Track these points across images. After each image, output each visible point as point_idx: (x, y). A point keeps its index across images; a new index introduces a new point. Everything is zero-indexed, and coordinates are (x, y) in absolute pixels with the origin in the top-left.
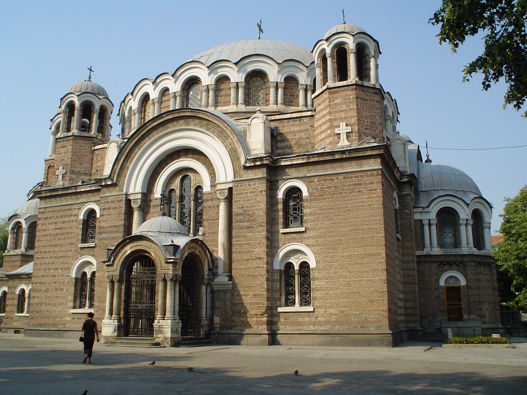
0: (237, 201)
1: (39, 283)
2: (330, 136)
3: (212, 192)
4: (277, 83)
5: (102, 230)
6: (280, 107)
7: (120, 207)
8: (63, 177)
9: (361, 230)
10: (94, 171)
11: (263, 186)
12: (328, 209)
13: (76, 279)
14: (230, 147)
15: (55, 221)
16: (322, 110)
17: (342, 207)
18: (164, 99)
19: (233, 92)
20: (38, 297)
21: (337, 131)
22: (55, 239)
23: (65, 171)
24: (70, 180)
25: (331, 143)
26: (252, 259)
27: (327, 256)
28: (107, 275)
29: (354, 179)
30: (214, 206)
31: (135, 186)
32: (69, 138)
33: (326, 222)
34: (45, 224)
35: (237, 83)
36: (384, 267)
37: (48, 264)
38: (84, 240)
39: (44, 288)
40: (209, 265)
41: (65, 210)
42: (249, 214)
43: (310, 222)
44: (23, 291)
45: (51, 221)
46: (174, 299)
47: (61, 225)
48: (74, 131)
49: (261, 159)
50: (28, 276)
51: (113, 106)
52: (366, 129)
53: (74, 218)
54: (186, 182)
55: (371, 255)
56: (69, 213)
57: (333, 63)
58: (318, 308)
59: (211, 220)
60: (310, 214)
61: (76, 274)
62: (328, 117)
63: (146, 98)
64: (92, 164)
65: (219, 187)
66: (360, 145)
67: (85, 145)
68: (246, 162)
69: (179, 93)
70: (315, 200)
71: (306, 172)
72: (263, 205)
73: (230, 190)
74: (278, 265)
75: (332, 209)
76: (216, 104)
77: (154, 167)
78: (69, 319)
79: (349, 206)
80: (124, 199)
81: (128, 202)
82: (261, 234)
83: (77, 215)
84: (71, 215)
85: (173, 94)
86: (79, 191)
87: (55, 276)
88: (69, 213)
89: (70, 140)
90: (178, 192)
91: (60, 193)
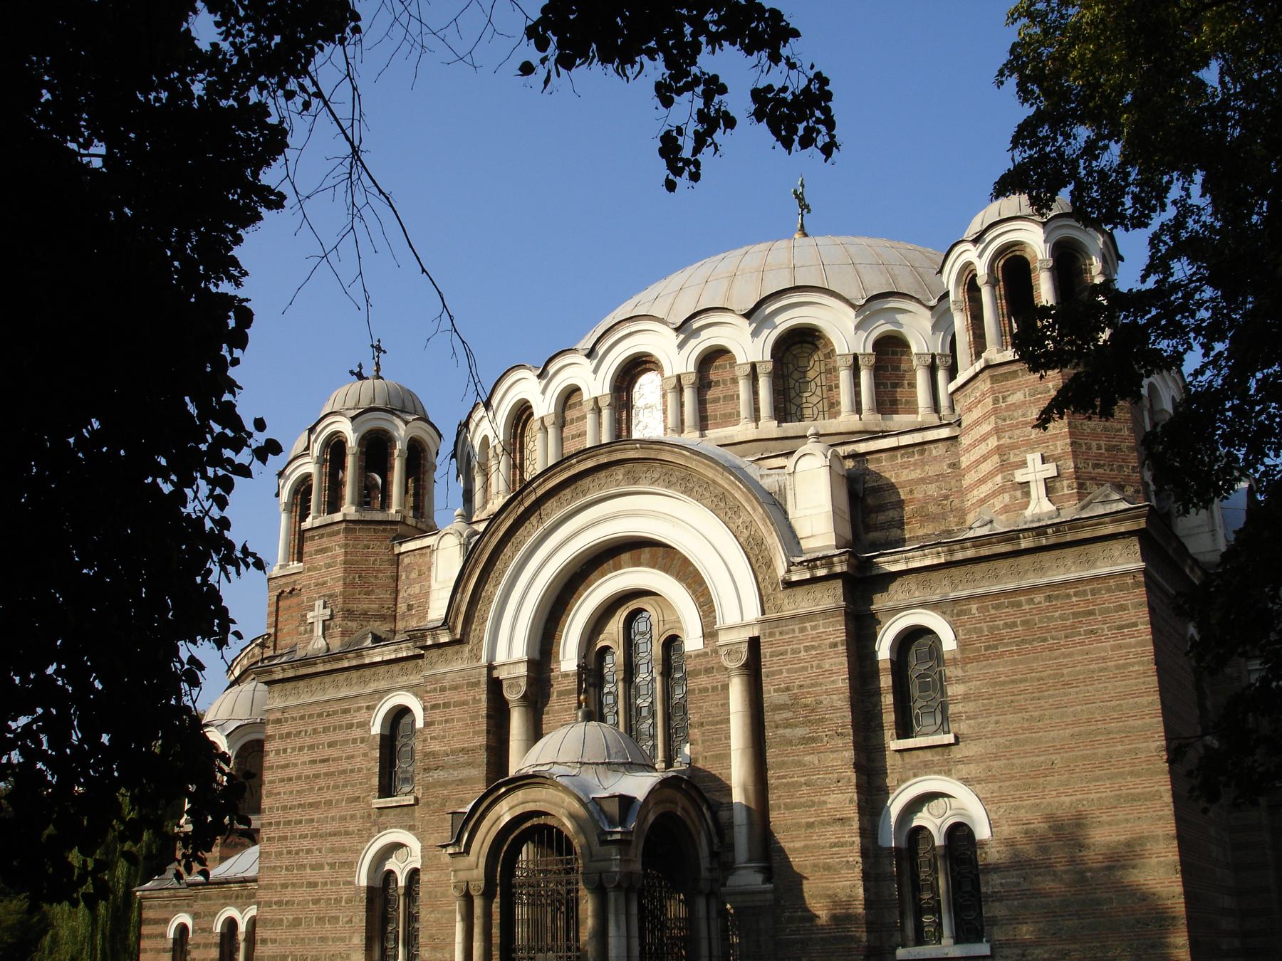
0: (773, 673)
1: (276, 903)
2: (1002, 490)
3: (708, 650)
4: (856, 357)
5: (432, 762)
6: (870, 418)
7: (475, 701)
8: (325, 628)
9: (1101, 734)
10: (402, 607)
11: (837, 631)
12: (1013, 681)
13: (370, 889)
14: (746, 533)
15: (309, 741)
16: (977, 423)
17: (1049, 676)
18: (569, 415)
19: (743, 389)
21: (1020, 476)
22: (312, 789)
23: (328, 611)
24: (343, 634)
25: (1006, 509)
26: (823, 823)
27: (1017, 808)
28: (453, 879)
29: (1074, 599)
30: (714, 689)
31: (511, 646)
32: (335, 528)
33: (1009, 717)
34: (285, 751)
35: (754, 366)
36: (1171, 829)
37: (297, 853)
38: (386, 789)
39: (288, 916)
40: (710, 843)
41: (335, 713)
42: (806, 706)
43: (968, 718)
44: (231, 924)
45: (298, 742)
46: (629, 937)
47: (326, 753)
48: (349, 509)
49: (827, 561)
50: (242, 888)
51: (440, 436)
52: (1096, 466)
53: (357, 733)
54: (640, 626)
55: (1135, 798)
56: (344, 720)
57: (994, 298)
58: (1001, 946)
59: (708, 723)
60: (966, 698)
61: (369, 878)
62: (993, 442)
63: (522, 412)
64: (397, 592)
65: (724, 638)
66: (1083, 508)
67: (376, 545)
68: (789, 571)
69: (608, 400)
70: (977, 659)
71: (948, 589)
72: (841, 681)
73: (754, 643)
74: (890, 840)
75: (1022, 681)
76: (703, 423)
77: (557, 592)
79: (1065, 671)
80: (484, 679)
81: (495, 686)
82: (842, 756)
83: (365, 725)
84: (350, 726)
85: (592, 403)
86: (367, 661)
87: (315, 885)
88: (344, 720)
89: (338, 533)
90: (619, 654)
91: (320, 668)
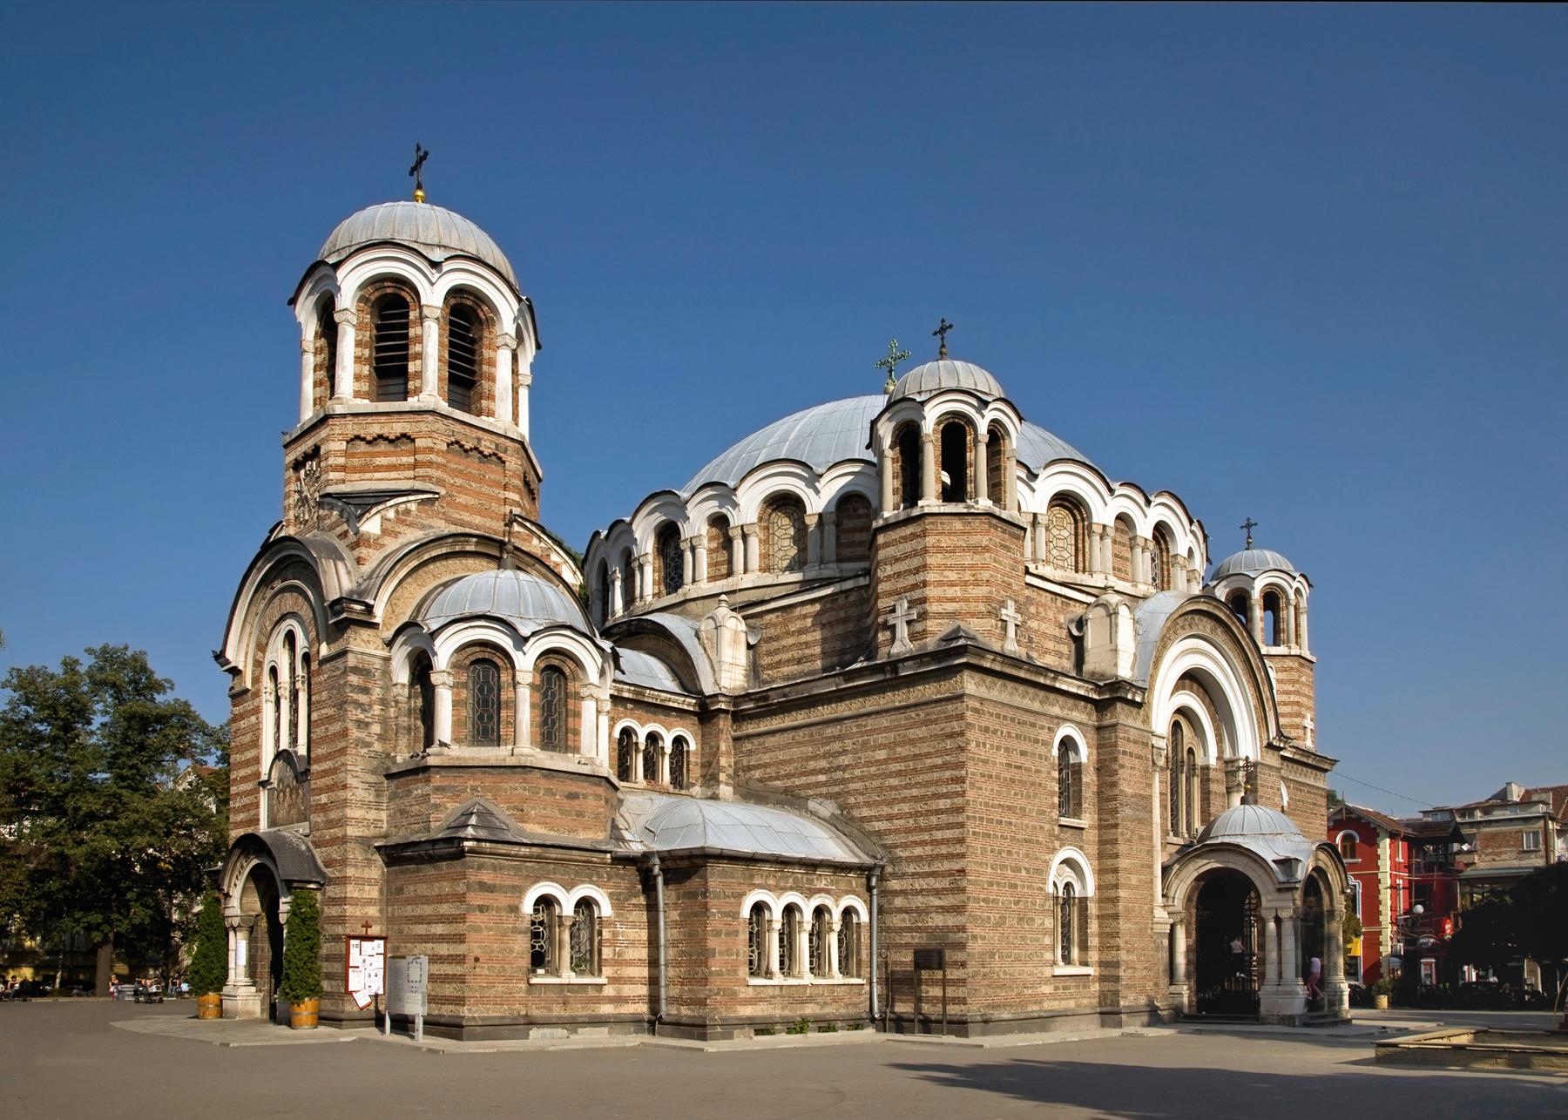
1: (984, 900)
20: (983, 938)
78: (1047, 989)
87: (1015, 886)
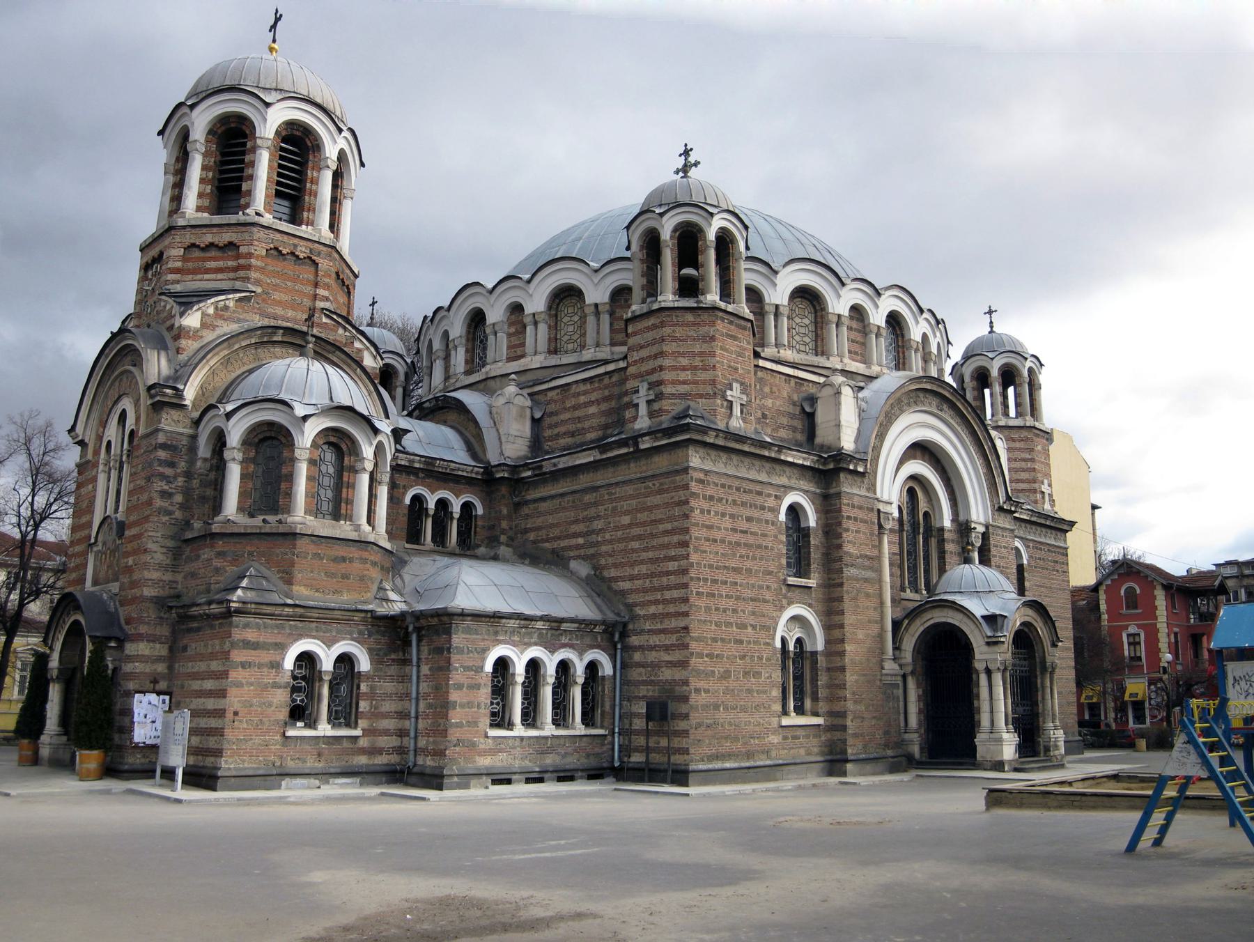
15: (729, 510)
22: (734, 555)
37: (725, 611)
39: (719, 670)
45: (721, 508)
47: (745, 525)
78: (775, 739)
87: (741, 642)
88: (758, 500)
